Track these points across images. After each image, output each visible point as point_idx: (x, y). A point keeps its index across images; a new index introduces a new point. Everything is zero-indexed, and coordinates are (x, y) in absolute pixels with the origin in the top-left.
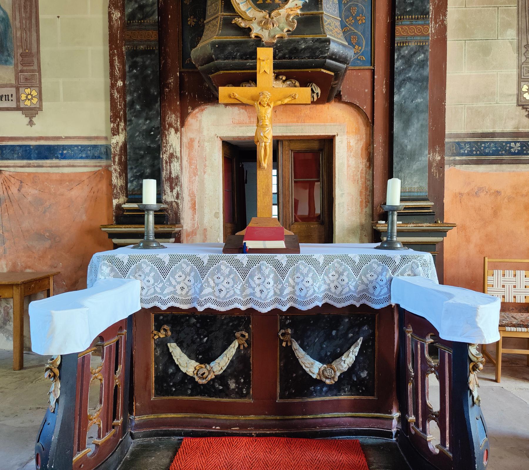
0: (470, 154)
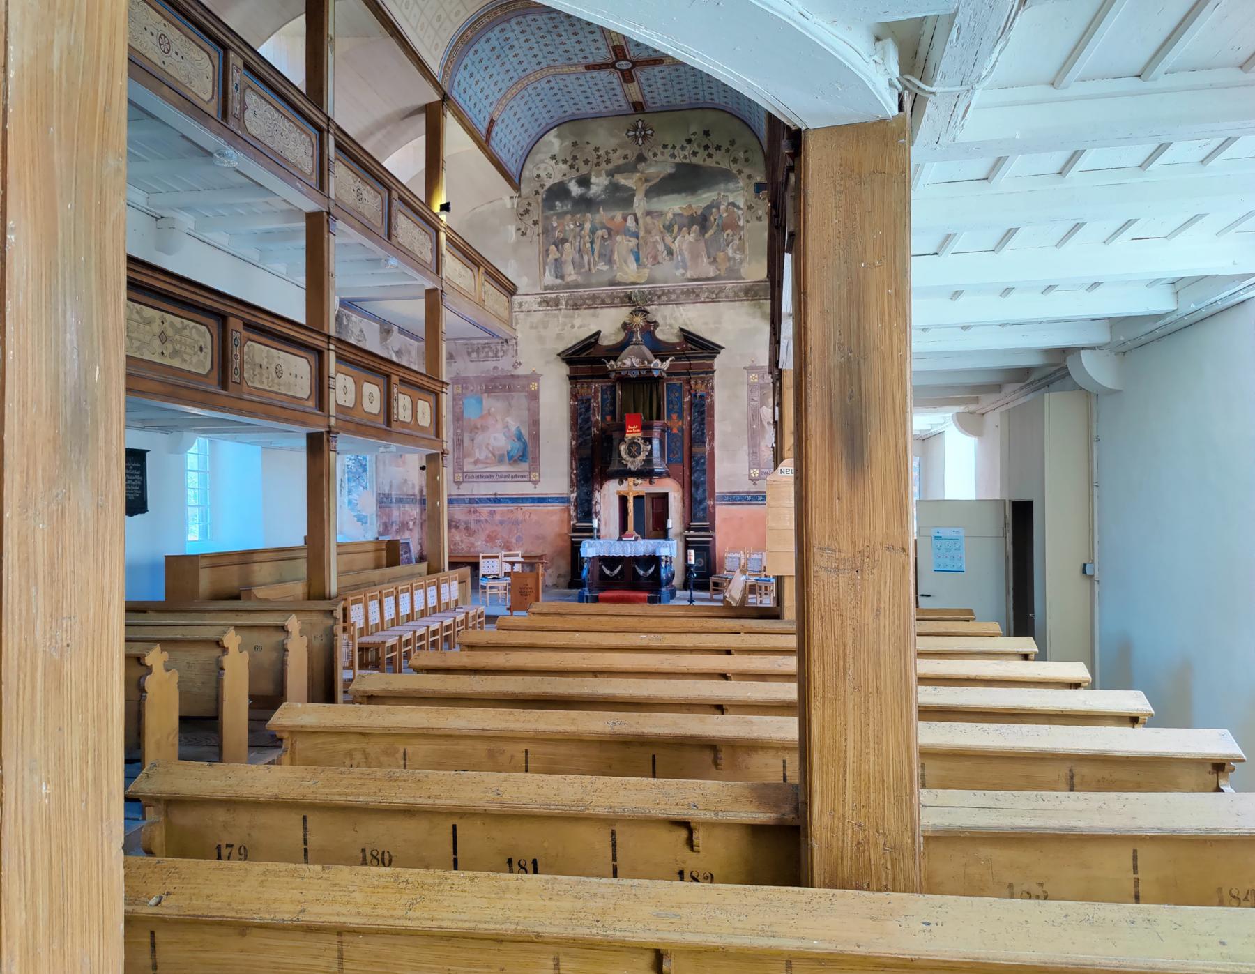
0: (729, 501)
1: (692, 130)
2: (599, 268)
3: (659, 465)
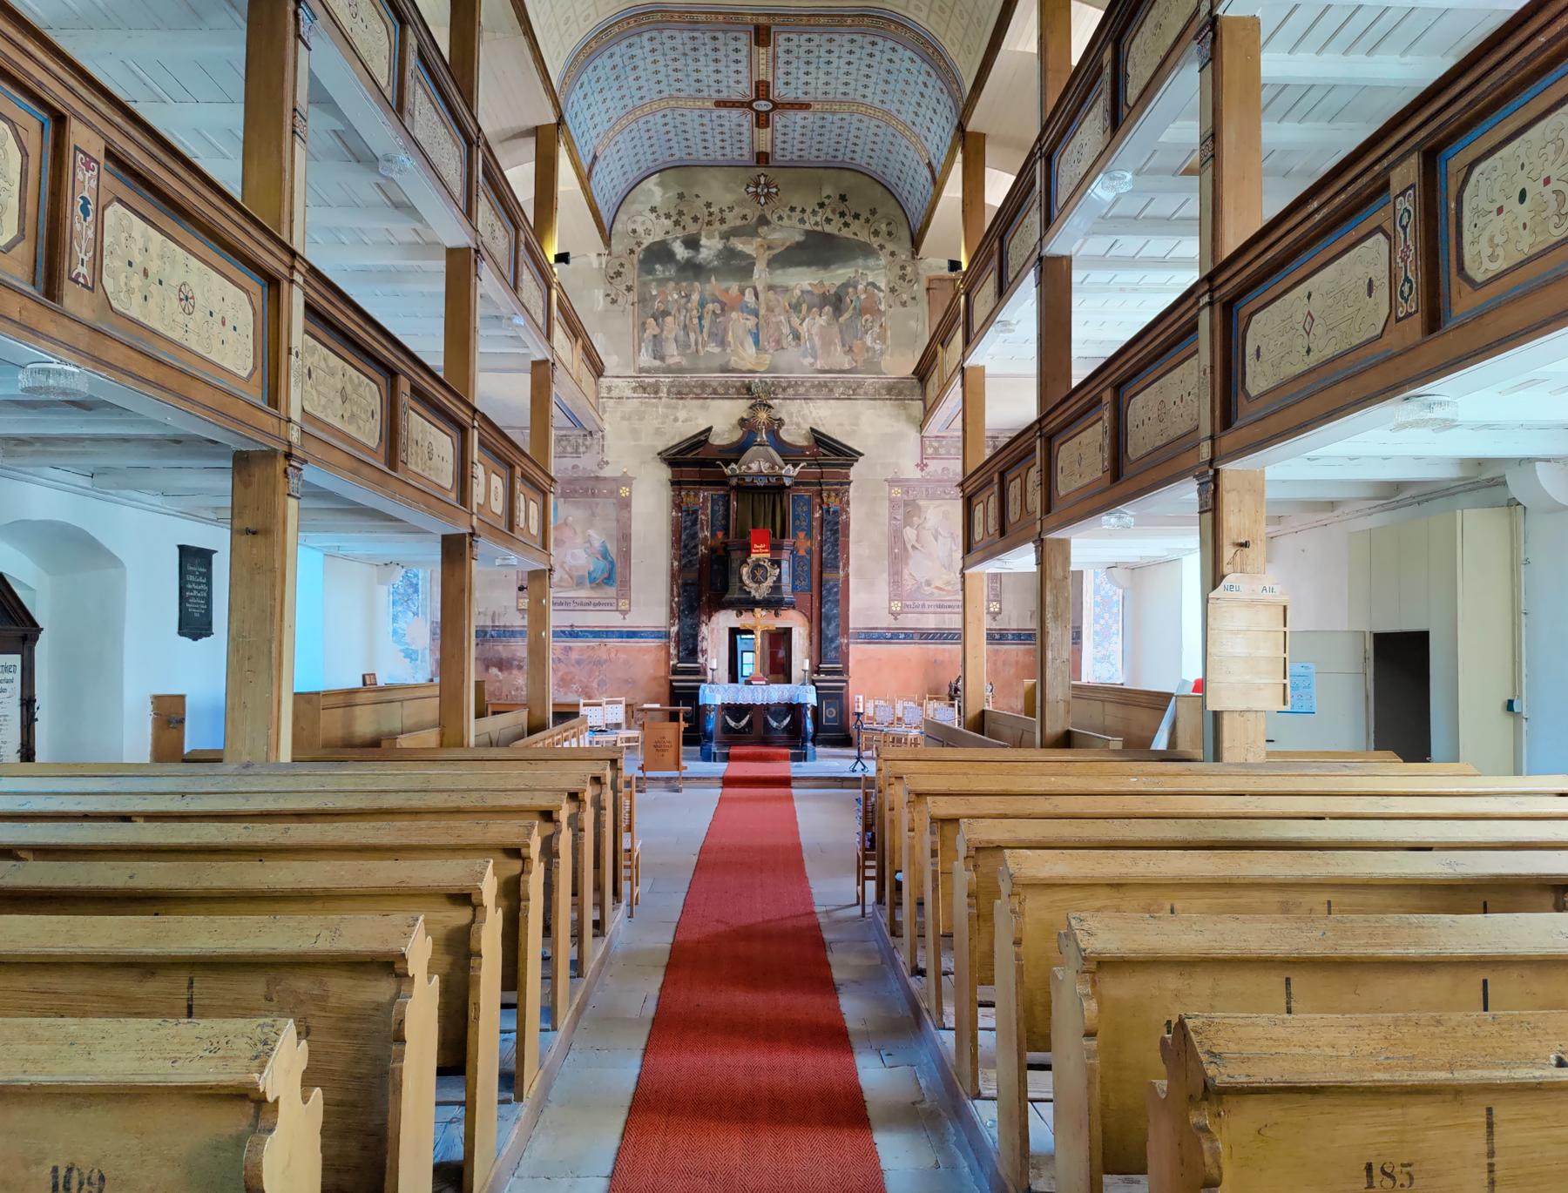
1: (827, 191)
2: (709, 349)
3: (787, 595)
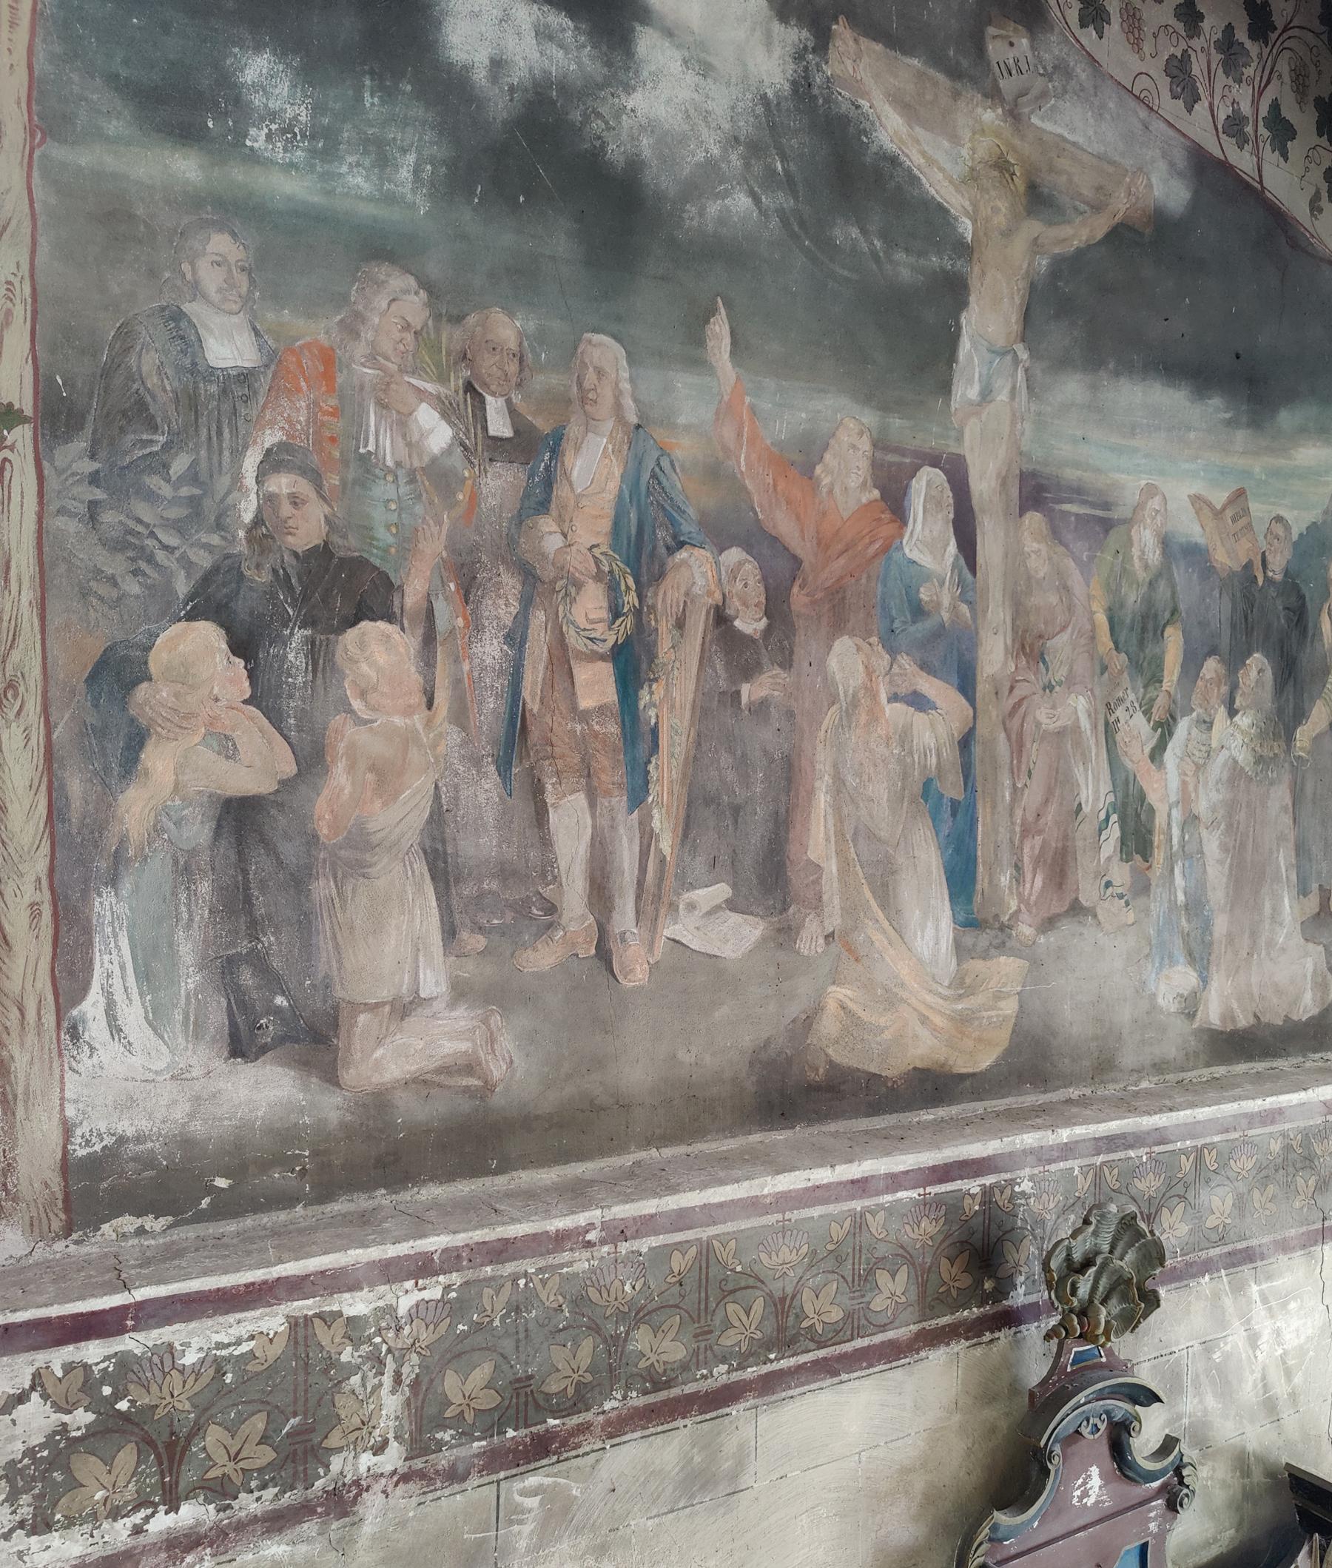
2: (682, 928)
